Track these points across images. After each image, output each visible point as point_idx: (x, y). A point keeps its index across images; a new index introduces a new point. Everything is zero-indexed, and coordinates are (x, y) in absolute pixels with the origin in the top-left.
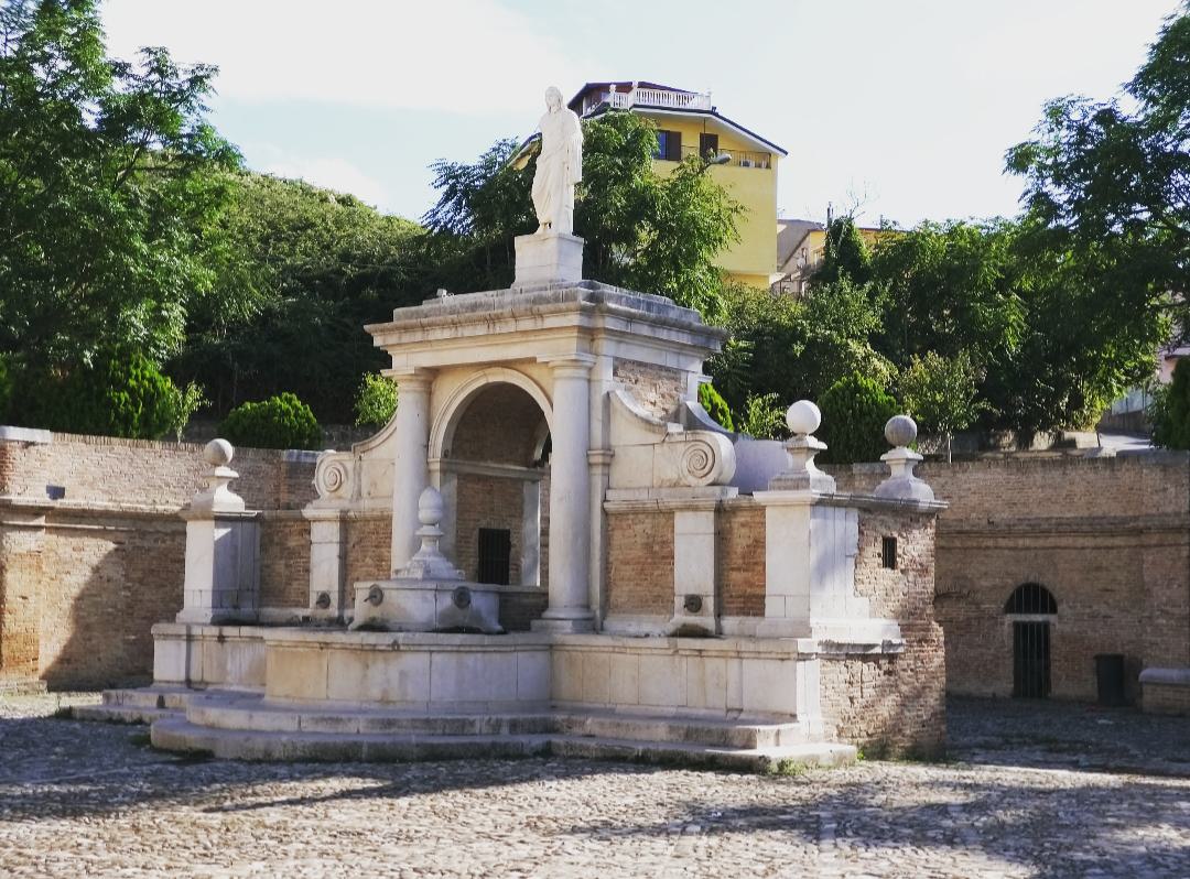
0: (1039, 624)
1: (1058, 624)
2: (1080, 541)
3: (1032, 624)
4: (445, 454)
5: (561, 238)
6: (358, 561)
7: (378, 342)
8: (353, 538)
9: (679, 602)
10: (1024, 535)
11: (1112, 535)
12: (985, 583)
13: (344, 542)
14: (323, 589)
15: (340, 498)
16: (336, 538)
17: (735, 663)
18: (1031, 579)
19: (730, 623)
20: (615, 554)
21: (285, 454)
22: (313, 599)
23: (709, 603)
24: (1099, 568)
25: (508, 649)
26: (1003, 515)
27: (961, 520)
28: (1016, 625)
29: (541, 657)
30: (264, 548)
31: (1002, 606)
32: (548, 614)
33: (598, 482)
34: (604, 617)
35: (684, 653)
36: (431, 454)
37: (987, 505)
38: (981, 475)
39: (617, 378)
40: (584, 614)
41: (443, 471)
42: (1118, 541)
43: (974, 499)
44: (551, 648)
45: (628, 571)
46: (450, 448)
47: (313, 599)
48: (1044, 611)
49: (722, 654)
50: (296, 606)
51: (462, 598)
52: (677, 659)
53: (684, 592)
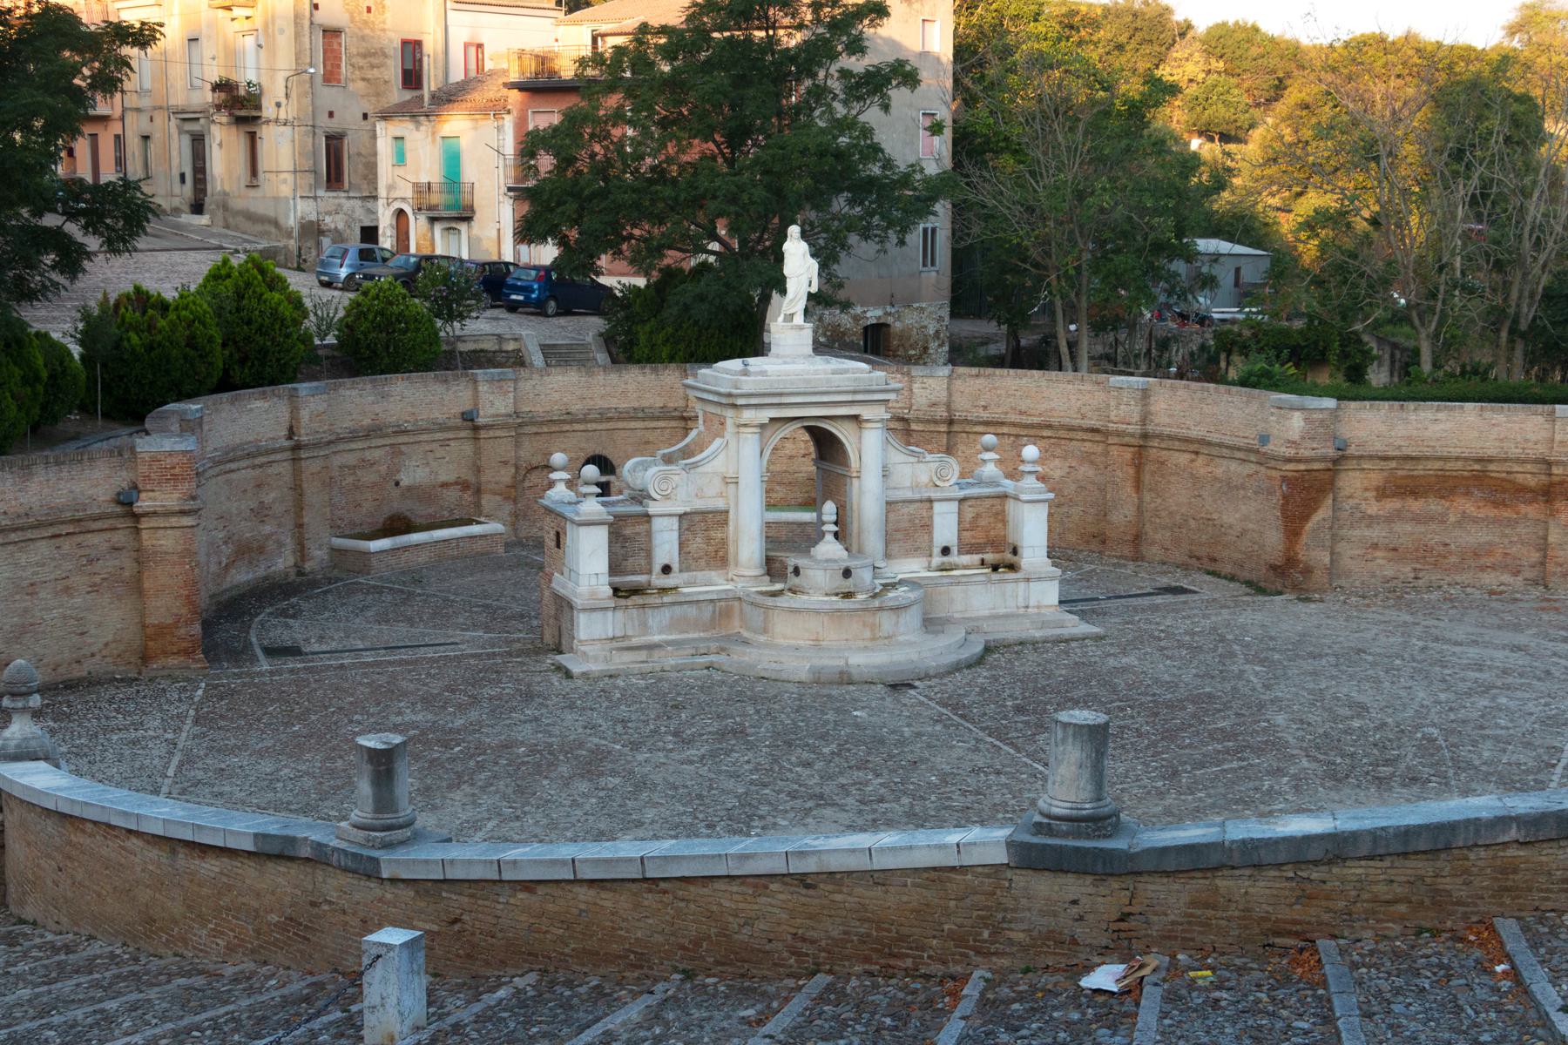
2: (633, 425)
9: (937, 551)
16: (676, 526)
17: (1022, 585)
19: (966, 559)
22: (657, 568)
23: (955, 550)
24: (647, 443)
26: (576, 407)
38: (560, 378)
42: (661, 424)
43: (556, 396)
47: (657, 568)
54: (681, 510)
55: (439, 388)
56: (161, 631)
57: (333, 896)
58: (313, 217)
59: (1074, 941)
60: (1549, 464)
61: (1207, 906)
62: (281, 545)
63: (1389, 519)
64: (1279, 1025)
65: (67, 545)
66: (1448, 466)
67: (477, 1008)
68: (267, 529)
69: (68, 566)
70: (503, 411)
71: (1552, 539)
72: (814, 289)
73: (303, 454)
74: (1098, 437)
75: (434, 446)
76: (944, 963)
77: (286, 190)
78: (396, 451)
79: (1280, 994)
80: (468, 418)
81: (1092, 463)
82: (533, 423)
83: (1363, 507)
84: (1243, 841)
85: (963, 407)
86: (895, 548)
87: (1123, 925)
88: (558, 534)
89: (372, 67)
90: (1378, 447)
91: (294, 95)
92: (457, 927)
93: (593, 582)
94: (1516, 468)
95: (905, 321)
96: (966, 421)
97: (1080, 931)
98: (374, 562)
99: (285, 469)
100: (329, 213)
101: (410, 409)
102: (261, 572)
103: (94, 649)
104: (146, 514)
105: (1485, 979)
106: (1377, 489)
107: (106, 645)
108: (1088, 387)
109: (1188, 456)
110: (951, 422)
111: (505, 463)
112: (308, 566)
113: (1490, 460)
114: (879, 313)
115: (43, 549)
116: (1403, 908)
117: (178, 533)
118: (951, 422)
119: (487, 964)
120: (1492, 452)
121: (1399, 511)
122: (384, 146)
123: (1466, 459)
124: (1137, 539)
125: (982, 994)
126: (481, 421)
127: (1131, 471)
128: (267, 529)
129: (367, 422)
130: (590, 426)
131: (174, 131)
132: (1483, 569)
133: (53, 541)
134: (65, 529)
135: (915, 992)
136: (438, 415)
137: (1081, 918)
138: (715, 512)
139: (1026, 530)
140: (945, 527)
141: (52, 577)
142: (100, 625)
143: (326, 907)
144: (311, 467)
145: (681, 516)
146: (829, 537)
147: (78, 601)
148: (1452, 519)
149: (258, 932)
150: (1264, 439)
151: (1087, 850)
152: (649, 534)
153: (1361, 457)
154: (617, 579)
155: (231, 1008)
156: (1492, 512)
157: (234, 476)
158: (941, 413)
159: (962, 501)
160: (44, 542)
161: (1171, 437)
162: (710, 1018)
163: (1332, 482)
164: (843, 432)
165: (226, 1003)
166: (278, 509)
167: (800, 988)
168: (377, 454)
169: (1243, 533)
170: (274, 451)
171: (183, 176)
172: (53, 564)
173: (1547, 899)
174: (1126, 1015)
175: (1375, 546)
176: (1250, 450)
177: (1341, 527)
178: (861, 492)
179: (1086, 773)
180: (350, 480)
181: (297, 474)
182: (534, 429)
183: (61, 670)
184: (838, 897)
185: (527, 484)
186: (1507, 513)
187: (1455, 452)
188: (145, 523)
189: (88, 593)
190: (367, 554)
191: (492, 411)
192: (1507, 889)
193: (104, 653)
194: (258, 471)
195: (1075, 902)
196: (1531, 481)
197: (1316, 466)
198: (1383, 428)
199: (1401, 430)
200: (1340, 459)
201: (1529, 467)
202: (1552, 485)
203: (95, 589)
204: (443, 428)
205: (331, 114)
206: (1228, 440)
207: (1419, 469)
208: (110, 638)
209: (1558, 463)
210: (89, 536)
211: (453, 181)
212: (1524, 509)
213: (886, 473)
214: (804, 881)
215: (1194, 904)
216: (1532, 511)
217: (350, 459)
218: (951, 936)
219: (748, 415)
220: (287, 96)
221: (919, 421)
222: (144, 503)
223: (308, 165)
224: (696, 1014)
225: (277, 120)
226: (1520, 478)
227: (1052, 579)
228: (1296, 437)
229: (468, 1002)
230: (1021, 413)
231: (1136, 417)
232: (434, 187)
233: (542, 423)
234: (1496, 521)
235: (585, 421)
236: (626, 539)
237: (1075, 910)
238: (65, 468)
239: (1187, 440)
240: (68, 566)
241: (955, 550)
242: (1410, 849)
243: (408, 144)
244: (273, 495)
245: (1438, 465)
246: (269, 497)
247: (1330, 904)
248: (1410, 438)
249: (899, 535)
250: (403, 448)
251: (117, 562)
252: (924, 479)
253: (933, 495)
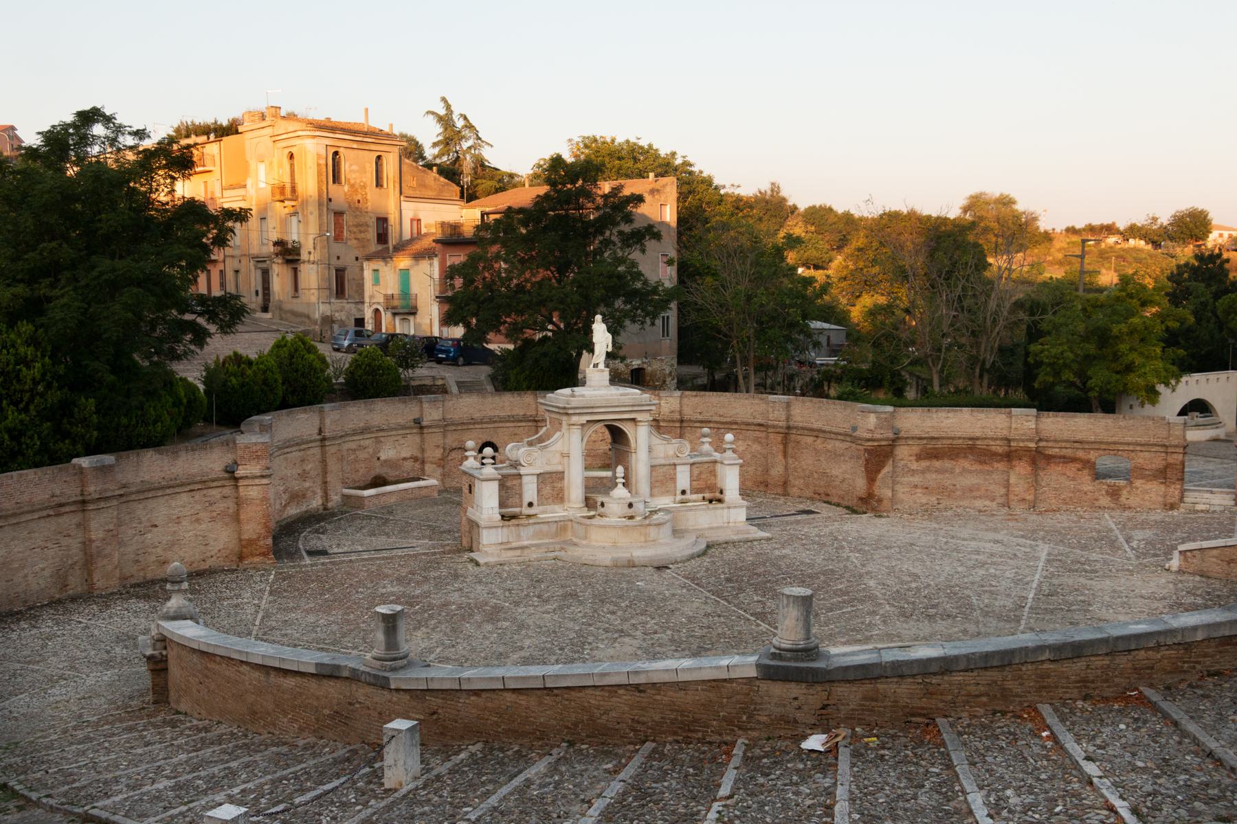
2: (508, 425)
9: (679, 492)
14: (530, 500)
16: (535, 481)
17: (726, 511)
19: (695, 497)
22: (525, 504)
26: (477, 415)
42: (523, 424)
43: (466, 409)
47: (525, 504)
54: (538, 472)
55: (401, 406)
56: (251, 542)
57: (361, 699)
58: (329, 313)
59: (796, 721)
60: (1009, 440)
61: (872, 700)
62: (314, 493)
63: (923, 472)
64: (921, 770)
65: (198, 495)
66: (954, 442)
67: (449, 765)
68: (307, 485)
70: (436, 418)
71: (1011, 481)
72: (610, 349)
73: (327, 443)
74: (762, 429)
75: (399, 437)
76: (720, 735)
77: (314, 299)
78: (378, 441)
79: (919, 751)
80: (417, 422)
81: (760, 442)
82: (453, 425)
83: (909, 465)
84: (893, 662)
85: (688, 413)
86: (656, 491)
87: (823, 712)
88: (470, 486)
89: (361, 232)
90: (916, 432)
91: (318, 248)
92: (435, 717)
93: (490, 512)
94: (992, 443)
95: (653, 367)
96: (690, 421)
97: (798, 715)
98: (366, 502)
99: (317, 451)
100: (337, 311)
102: (304, 508)
103: (213, 553)
104: (242, 478)
105: (1037, 741)
106: (916, 455)
108: (757, 401)
109: (812, 438)
110: (682, 421)
111: (438, 446)
112: (330, 505)
113: (977, 439)
114: (639, 362)
115: (185, 498)
116: (984, 699)
117: (260, 488)
118: (682, 421)
119: (453, 738)
120: (978, 434)
121: (928, 467)
122: (368, 274)
123: (964, 438)
124: (785, 484)
125: (745, 753)
126: (424, 423)
127: (781, 447)
128: (307, 485)
129: (362, 425)
130: (484, 426)
131: (252, 268)
132: (975, 498)
134: (196, 487)
135: (704, 752)
136: (401, 421)
137: (800, 708)
138: (556, 473)
139: (727, 480)
140: (683, 479)
142: (216, 540)
143: (358, 706)
144: (331, 450)
145: (538, 475)
146: (620, 486)
147: (203, 526)
148: (957, 471)
149: (317, 720)
150: (854, 429)
151: (803, 668)
152: (521, 485)
153: (907, 438)
154: (504, 510)
155: (304, 765)
156: (977, 467)
157: (289, 455)
158: (677, 416)
159: (692, 464)
161: (803, 428)
162: (586, 770)
163: (892, 452)
164: (627, 428)
165: (301, 762)
166: (313, 473)
167: (637, 751)
168: (367, 442)
169: (843, 480)
170: (311, 442)
171: (257, 292)
173: (1067, 692)
174: (830, 765)
175: (916, 486)
176: (846, 435)
177: (897, 476)
178: (637, 460)
179: (801, 624)
180: (353, 457)
181: (324, 454)
182: (454, 428)
183: (194, 565)
184: (658, 697)
185: (450, 458)
186: (987, 467)
187: (958, 434)
188: (241, 483)
190: (362, 498)
191: (431, 418)
192: (1044, 687)
194: (302, 452)
195: (796, 699)
196: (1000, 450)
197: (883, 443)
198: (919, 422)
199: (928, 423)
200: (896, 440)
201: (998, 442)
202: (1011, 452)
203: (213, 520)
204: (404, 428)
205: (338, 258)
206: (834, 429)
207: (939, 444)
208: (222, 547)
209: (1014, 440)
211: (405, 294)
212: (996, 465)
213: (650, 450)
214: (638, 688)
215: (864, 698)
216: (1000, 466)
217: (353, 445)
218: (724, 719)
219: (575, 419)
220: (314, 248)
221: (664, 421)
222: (240, 472)
223: (326, 285)
224: (579, 767)
225: (309, 261)
226: (993, 448)
227: (742, 507)
228: (872, 427)
229: (443, 761)
230: (720, 416)
231: (784, 418)
232: (395, 297)
233: (458, 424)
234: (981, 471)
235: (482, 423)
236: (508, 488)
237: (796, 703)
238: (197, 453)
239: (812, 430)
241: (688, 492)
242: (988, 665)
243: (381, 274)
244: (310, 466)
245: (949, 442)
246: (308, 467)
247: (944, 698)
248: (933, 427)
249: (657, 484)
250: (382, 439)
251: (225, 505)
252: (671, 453)
253: (676, 461)
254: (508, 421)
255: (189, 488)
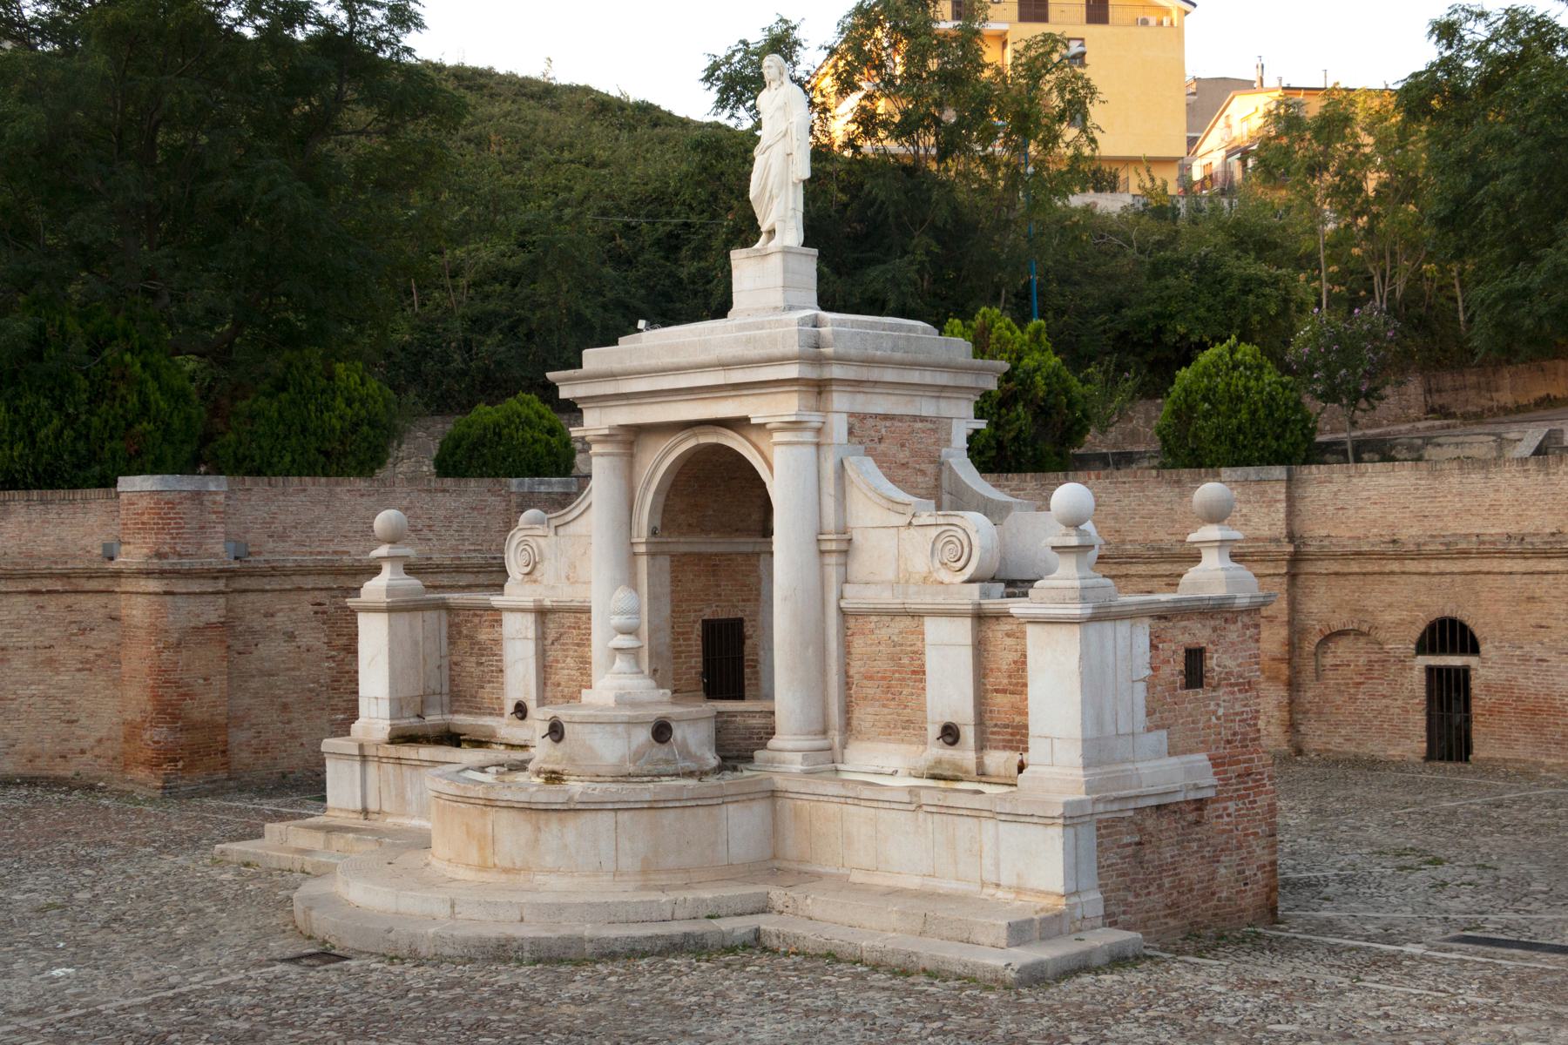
0: (1457, 670)
1: (1484, 670)
2: (1508, 565)
3: (1449, 669)
4: (654, 532)
5: (786, 251)
6: (557, 661)
7: (565, 393)
8: (552, 635)
9: (934, 731)
10: (1436, 556)
11: (1546, 555)
12: (1389, 617)
13: (541, 637)
15: (535, 581)
16: (531, 633)
18: (1447, 613)
20: (856, 668)
21: (514, 481)
23: (968, 734)
24: (1531, 599)
25: (714, 801)
26: (1410, 532)
27: (1359, 538)
28: (1430, 670)
29: (759, 809)
30: (452, 641)
31: (1413, 646)
32: (772, 743)
33: (833, 574)
34: (844, 746)
35: (929, 809)
36: (635, 533)
37: (1391, 518)
38: (1382, 480)
39: (854, 440)
40: (820, 743)
41: (652, 555)
43: (1375, 511)
44: (773, 794)
45: (871, 689)
46: (658, 523)
48: (1463, 651)
49: (974, 813)
50: (491, 714)
51: (662, 731)
52: (921, 815)
53: (938, 719)
65: (53, 605)
69: (53, 632)
70: (1265, 532)
82: (1333, 557)
101: (1112, 523)
103: (85, 744)
107: (100, 741)
130: (1434, 566)
133: (35, 598)
141: (30, 643)
142: (91, 715)
147: (65, 678)
160: (22, 598)
172: (35, 627)
182: (1335, 567)
183: (40, 763)
185: (1329, 660)
189: (79, 670)
193: (97, 751)
203: (86, 666)
208: (103, 733)
210: (82, 597)
233: (1345, 556)
235: (1418, 555)
238: (54, 508)
240: (53, 632)
241: (968, 734)
251: (113, 636)
254: (1505, 554)
255: (31, 585)
